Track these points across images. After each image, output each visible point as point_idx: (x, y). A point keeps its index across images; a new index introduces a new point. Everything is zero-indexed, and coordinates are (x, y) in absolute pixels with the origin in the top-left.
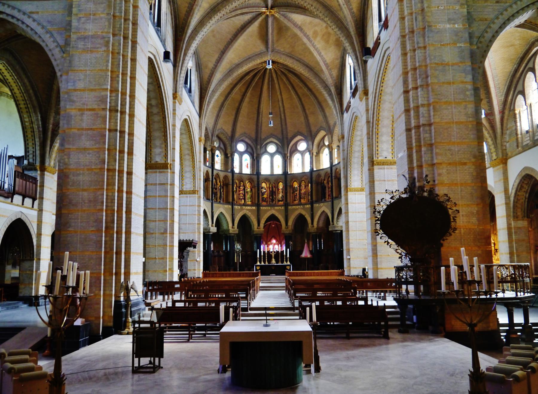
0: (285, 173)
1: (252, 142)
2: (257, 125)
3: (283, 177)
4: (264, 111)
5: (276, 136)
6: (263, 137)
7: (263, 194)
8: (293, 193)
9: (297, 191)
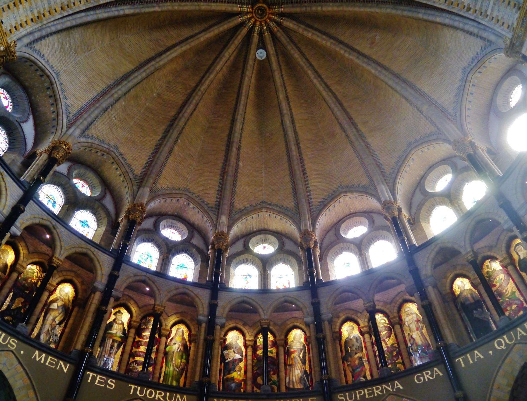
0: (313, 284)
1: (206, 212)
2: (224, 173)
3: (305, 298)
4: (243, 150)
5: (276, 205)
6: (239, 205)
7: (228, 367)
8: (344, 359)
9: (360, 349)
